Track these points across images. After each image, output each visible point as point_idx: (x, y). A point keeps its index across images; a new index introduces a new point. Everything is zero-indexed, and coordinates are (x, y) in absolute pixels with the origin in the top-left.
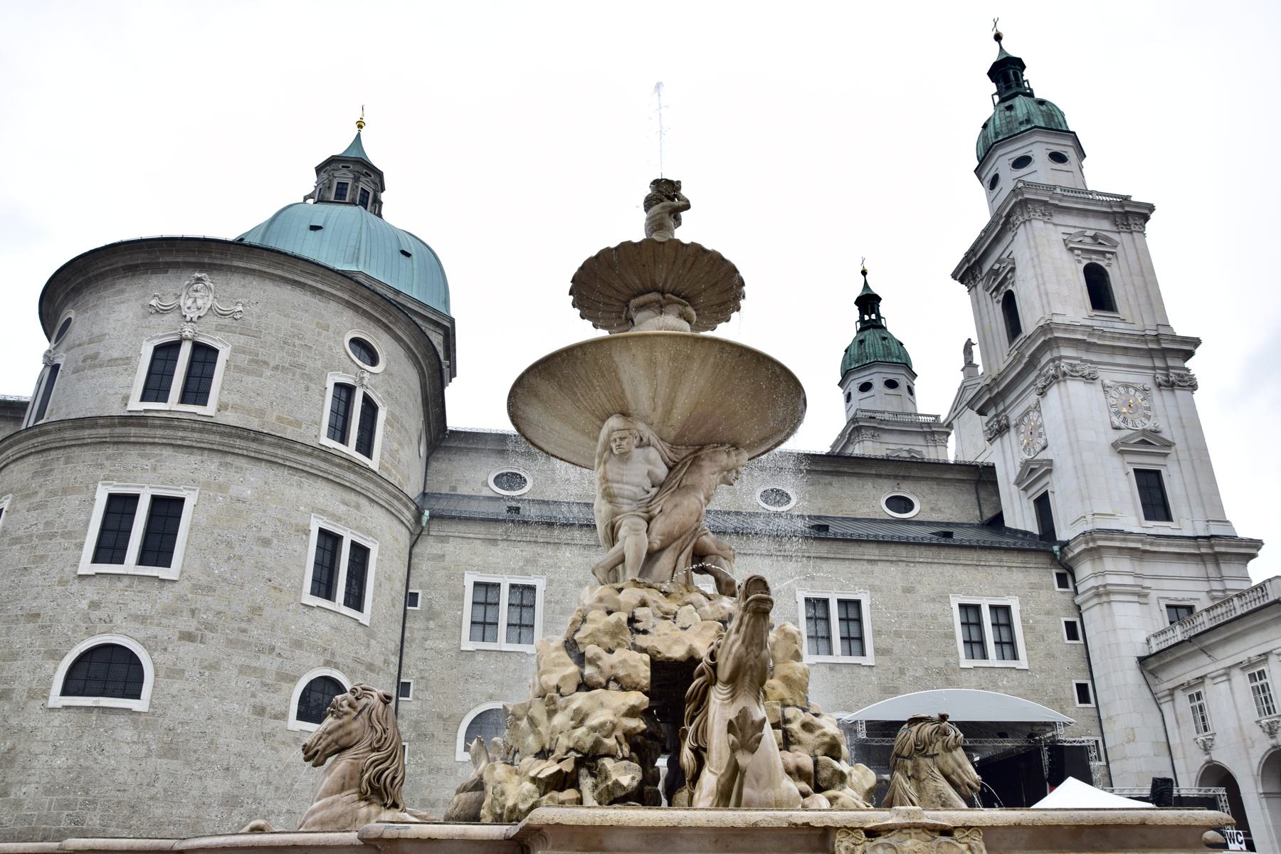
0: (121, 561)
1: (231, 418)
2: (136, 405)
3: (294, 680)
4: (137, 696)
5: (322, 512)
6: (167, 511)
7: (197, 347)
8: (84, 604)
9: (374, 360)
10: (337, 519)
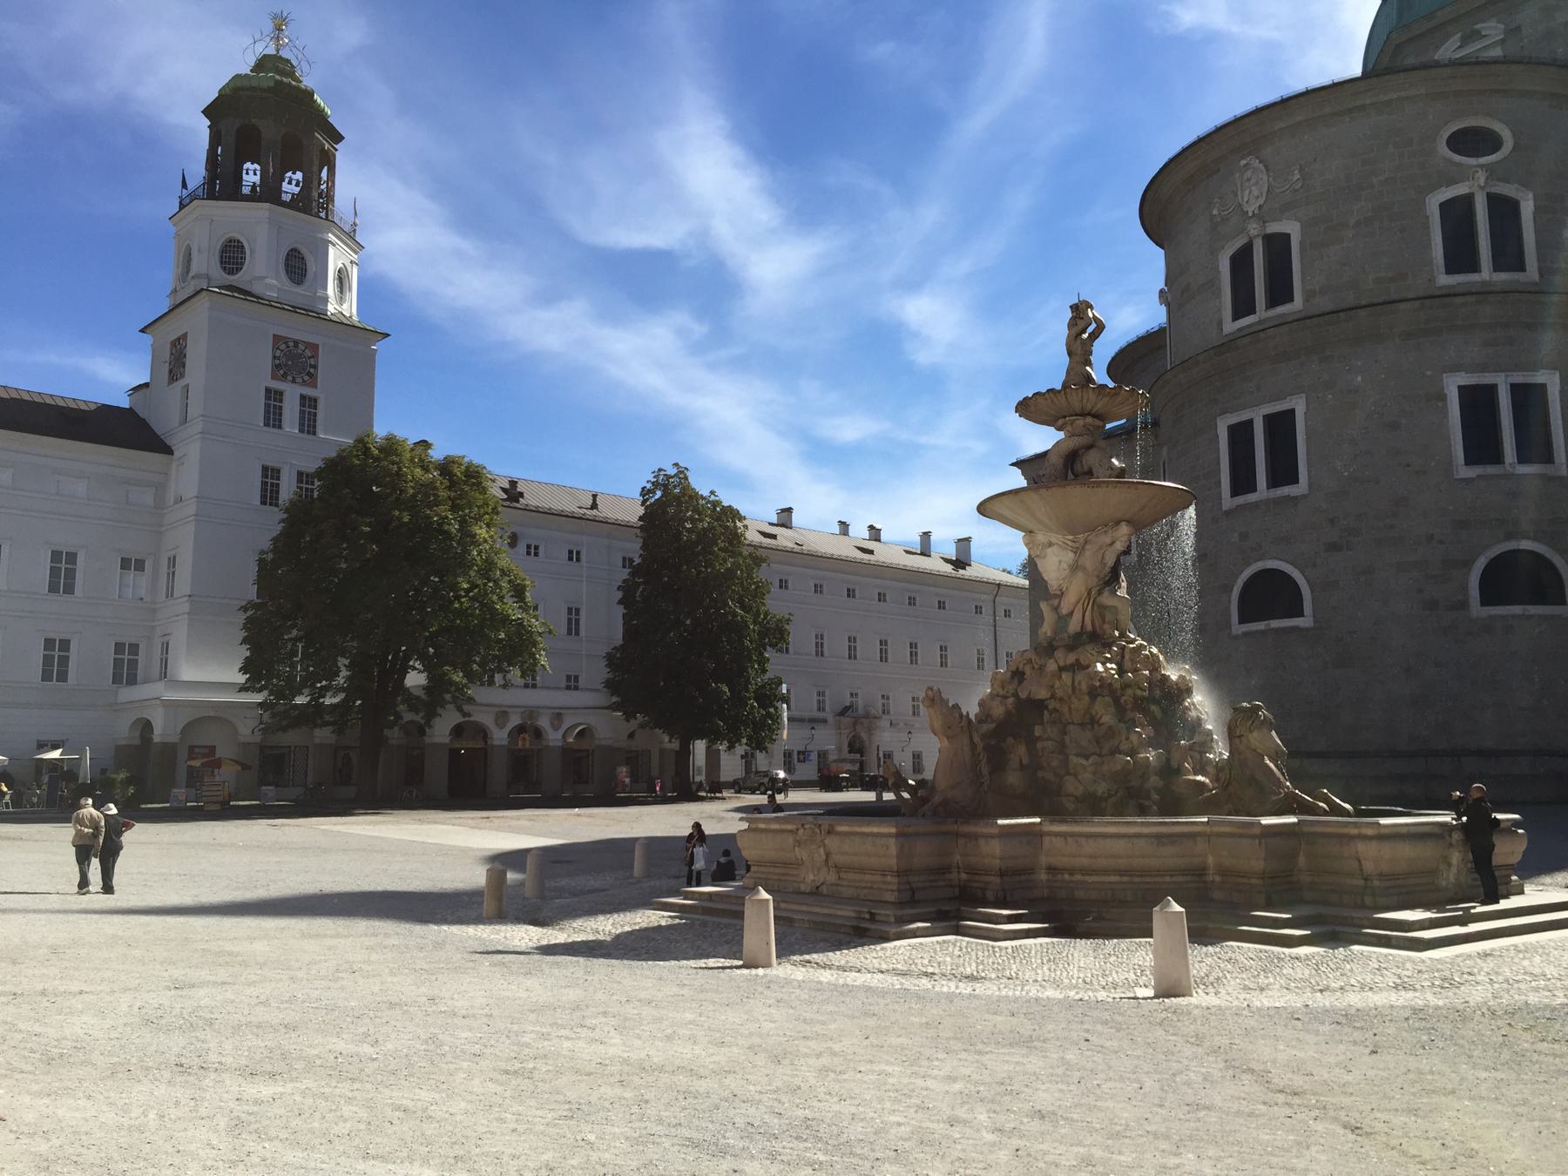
0: (1255, 490)
1: (1324, 303)
2: (1230, 327)
3: (1468, 564)
4: (1301, 614)
5: (1455, 368)
6: (1281, 426)
7: (1269, 239)
8: (1235, 538)
9: (1494, 143)
10: (1483, 368)
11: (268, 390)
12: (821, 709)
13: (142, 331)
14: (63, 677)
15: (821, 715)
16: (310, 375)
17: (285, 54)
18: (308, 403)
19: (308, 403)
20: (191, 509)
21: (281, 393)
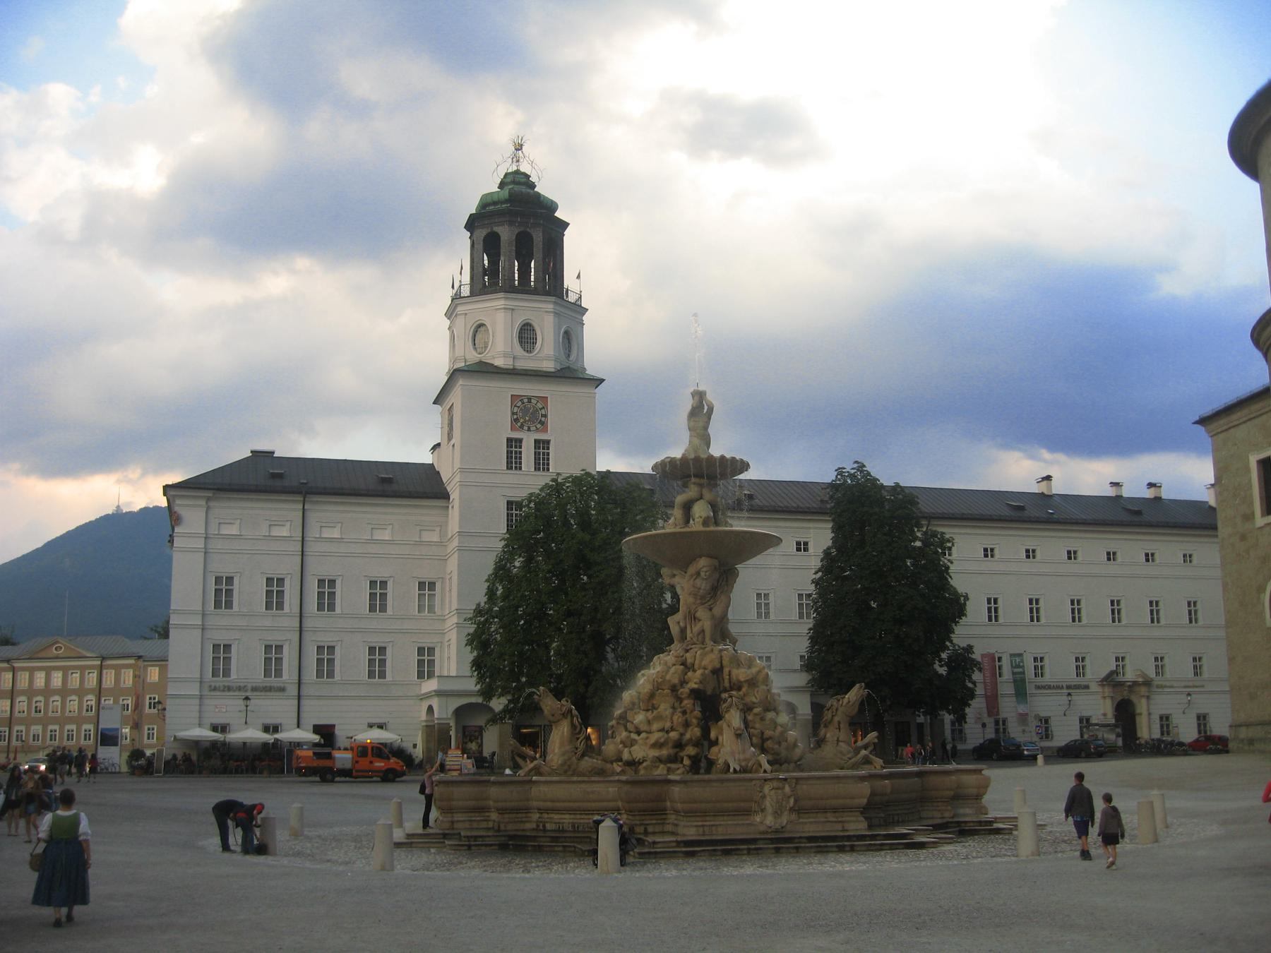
11: (509, 440)
12: (1080, 671)
13: (435, 403)
14: (382, 675)
15: (1080, 681)
16: (542, 423)
17: (525, 168)
18: (542, 445)
19: (542, 445)
20: (455, 543)
21: (521, 441)
